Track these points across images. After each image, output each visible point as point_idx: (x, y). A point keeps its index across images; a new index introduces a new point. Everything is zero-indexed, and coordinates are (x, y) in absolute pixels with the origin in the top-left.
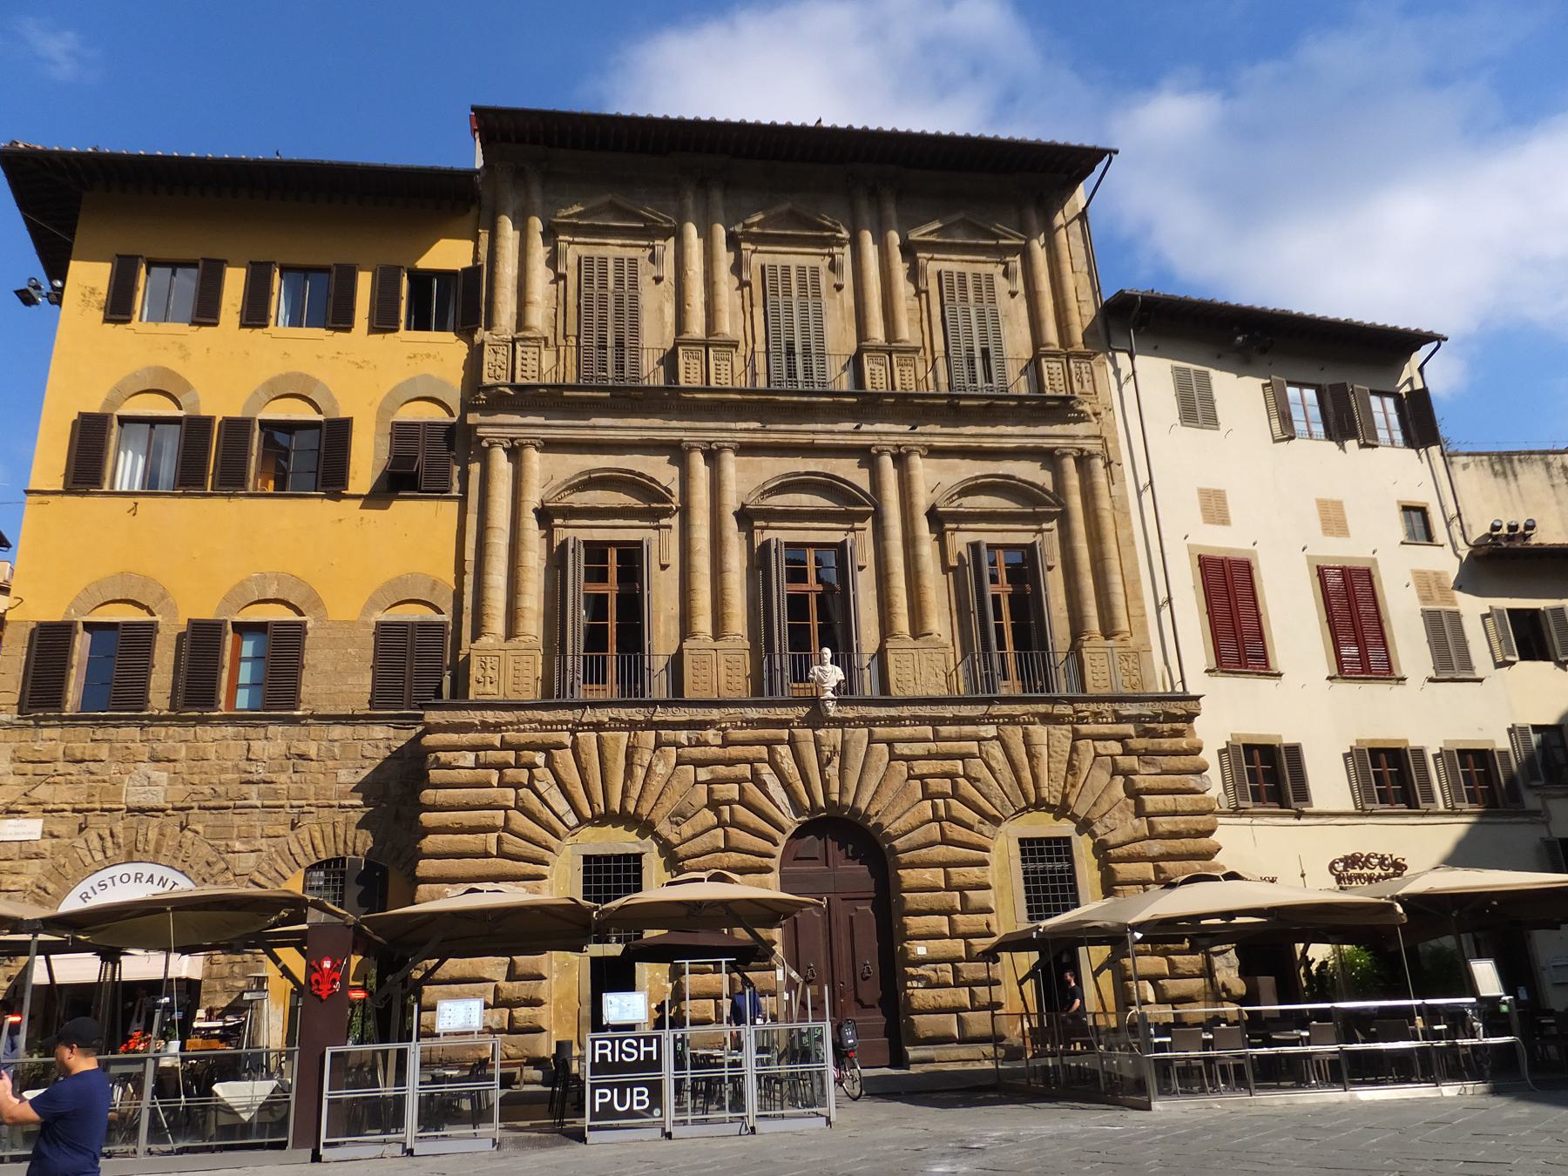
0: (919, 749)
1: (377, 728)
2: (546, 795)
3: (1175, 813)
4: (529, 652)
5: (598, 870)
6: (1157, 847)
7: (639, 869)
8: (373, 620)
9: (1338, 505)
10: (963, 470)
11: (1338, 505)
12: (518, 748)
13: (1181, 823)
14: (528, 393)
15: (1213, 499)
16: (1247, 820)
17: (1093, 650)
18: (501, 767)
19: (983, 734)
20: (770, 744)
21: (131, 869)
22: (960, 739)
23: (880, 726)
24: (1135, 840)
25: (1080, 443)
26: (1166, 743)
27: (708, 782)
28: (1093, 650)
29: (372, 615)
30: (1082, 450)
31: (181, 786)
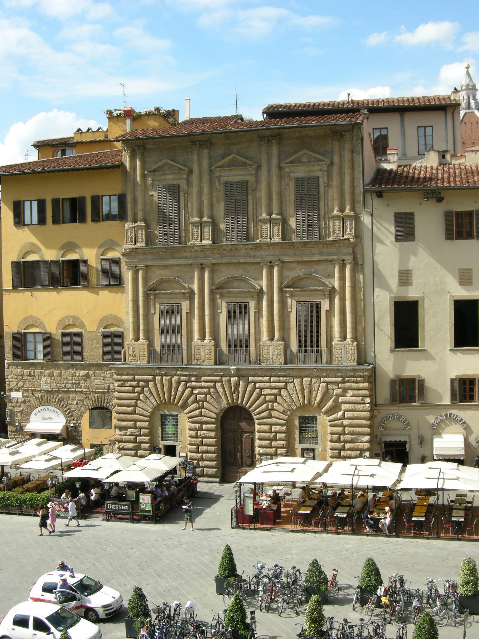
0: (263, 385)
1: (105, 367)
2: (148, 396)
3: (355, 411)
4: (144, 346)
5: (165, 419)
6: (346, 422)
7: (177, 419)
8: (101, 331)
9: (469, 271)
10: (298, 269)
11: (469, 271)
12: (139, 381)
13: (356, 414)
14: (138, 250)
15: (405, 274)
16: (396, 408)
17: (337, 346)
18: (134, 387)
19: (287, 380)
20: (215, 382)
21: (46, 407)
22: (280, 382)
23: (253, 376)
24: (338, 419)
25: (343, 258)
26: (354, 385)
27: (196, 394)
28: (337, 346)
29: (100, 329)
30: (343, 260)
31: (55, 384)
